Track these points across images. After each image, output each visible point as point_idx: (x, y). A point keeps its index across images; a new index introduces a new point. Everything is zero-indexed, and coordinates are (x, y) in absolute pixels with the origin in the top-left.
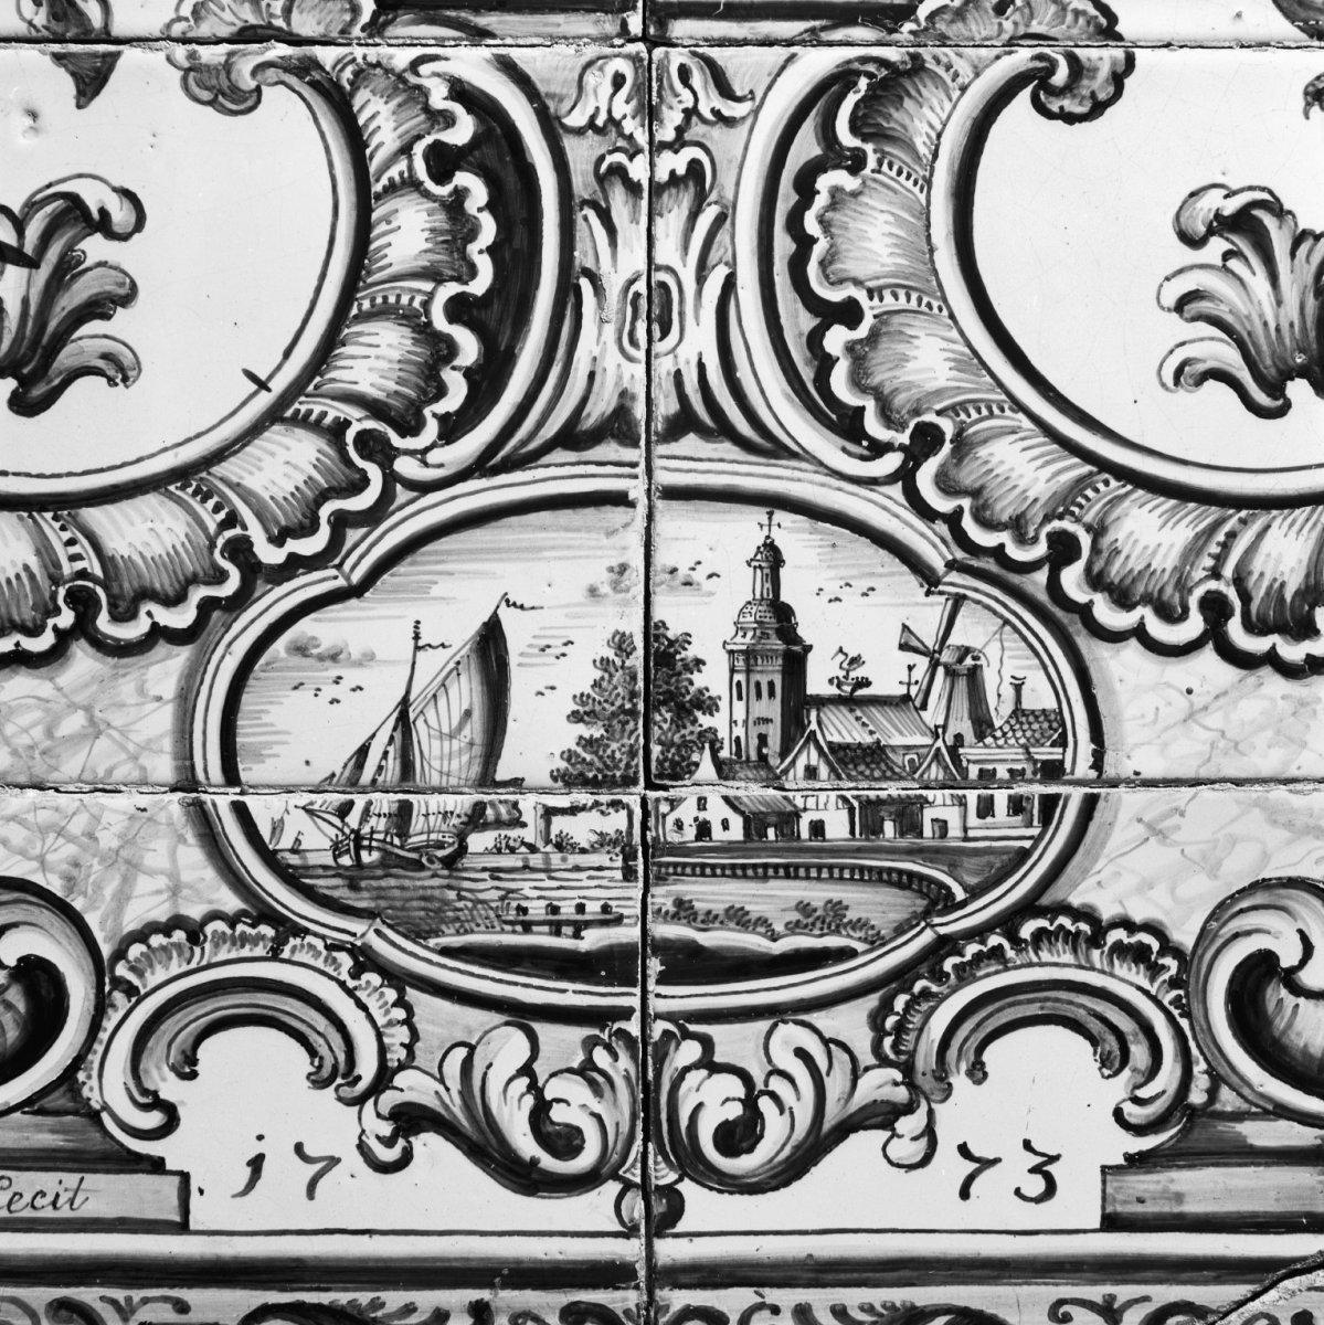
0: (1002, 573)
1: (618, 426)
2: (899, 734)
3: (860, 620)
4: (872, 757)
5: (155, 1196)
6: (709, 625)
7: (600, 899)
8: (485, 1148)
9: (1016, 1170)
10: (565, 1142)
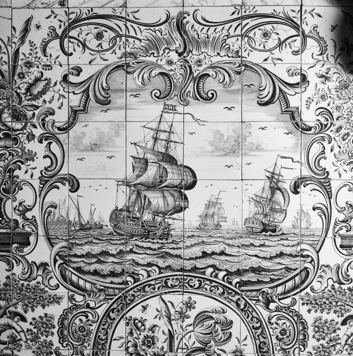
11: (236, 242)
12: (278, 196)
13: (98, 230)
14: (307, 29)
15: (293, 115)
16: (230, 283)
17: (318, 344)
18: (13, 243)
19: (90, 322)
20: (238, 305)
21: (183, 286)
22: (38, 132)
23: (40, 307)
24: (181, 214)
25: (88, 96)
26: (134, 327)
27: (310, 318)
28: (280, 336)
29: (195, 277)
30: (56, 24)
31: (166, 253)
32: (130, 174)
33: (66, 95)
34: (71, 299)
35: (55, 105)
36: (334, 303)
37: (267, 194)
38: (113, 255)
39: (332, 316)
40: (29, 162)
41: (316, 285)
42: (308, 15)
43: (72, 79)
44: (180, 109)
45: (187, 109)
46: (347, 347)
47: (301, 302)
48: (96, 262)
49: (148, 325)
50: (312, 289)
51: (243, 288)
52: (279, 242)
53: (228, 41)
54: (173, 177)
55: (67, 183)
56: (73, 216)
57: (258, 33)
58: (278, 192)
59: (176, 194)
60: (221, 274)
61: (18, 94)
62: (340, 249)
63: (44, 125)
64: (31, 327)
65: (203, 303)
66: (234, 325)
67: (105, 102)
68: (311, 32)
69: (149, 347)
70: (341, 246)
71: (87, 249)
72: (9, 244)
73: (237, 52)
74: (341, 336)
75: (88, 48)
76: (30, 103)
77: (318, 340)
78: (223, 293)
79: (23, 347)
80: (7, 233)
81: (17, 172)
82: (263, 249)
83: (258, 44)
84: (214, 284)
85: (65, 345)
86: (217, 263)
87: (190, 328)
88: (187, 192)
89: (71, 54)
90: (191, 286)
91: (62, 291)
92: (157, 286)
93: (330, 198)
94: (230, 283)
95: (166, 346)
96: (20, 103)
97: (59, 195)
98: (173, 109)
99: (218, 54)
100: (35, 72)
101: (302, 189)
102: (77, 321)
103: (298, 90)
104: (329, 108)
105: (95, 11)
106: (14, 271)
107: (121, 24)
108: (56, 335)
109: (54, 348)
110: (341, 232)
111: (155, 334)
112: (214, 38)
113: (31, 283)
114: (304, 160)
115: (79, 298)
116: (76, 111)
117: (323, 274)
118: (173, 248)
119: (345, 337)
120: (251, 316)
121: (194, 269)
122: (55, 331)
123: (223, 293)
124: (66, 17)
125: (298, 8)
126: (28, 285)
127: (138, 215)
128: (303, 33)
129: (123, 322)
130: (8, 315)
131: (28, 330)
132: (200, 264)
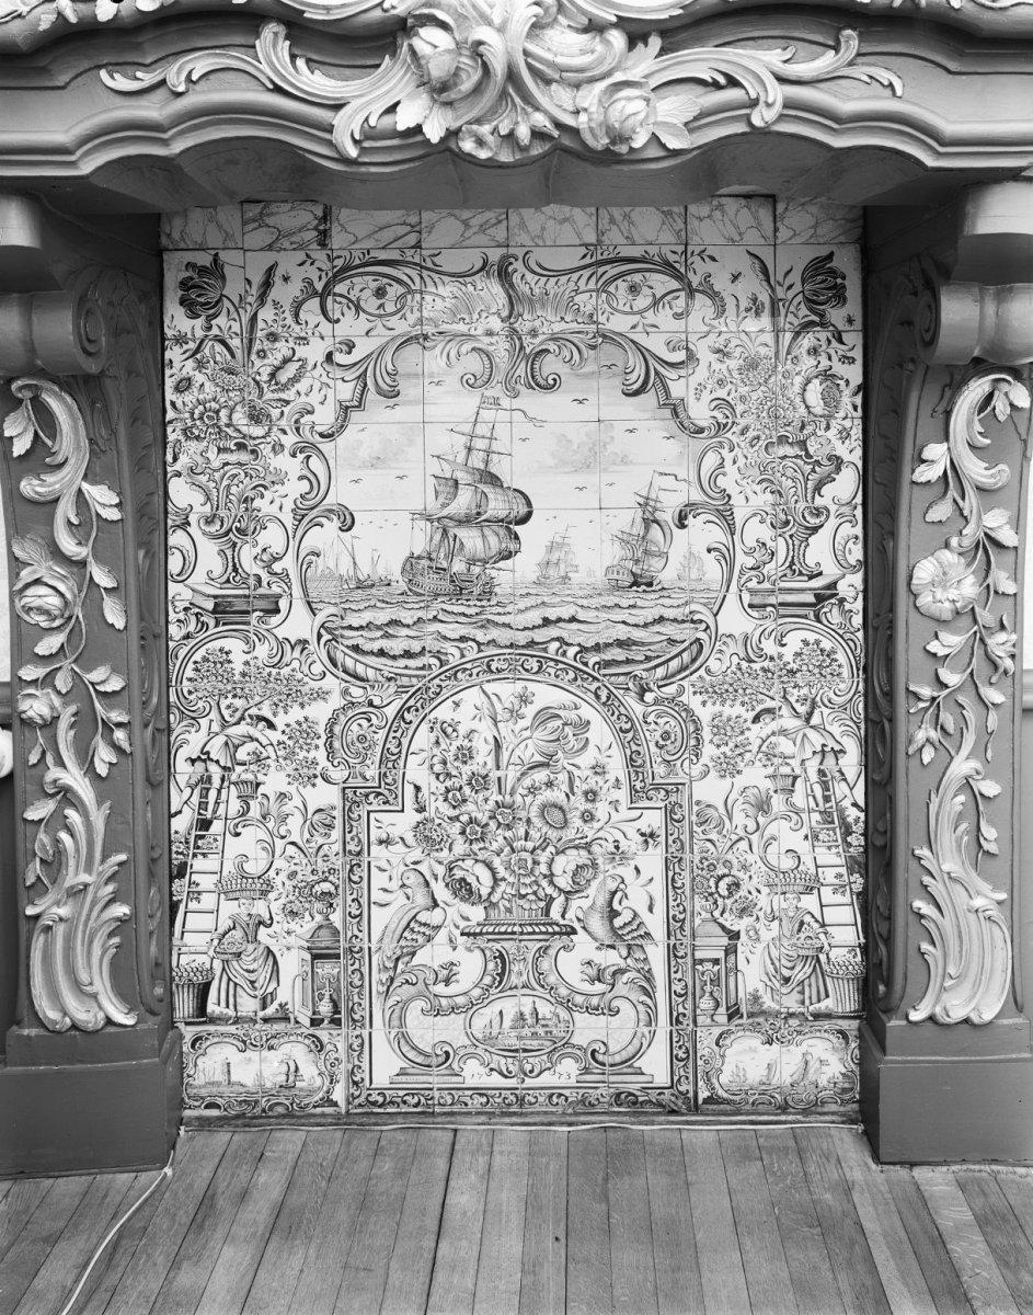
0: (562, 1004)
1: (516, 987)
2: (549, 1023)
3: (545, 1010)
4: (547, 1026)
5: (459, 1079)
6: (527, 1011)
7: (515, 1043)
8: (501, 1073)
9: (565, 1075)
10: (510, 1072)
11: (595, 602)
12: (655, 530)
13: (384, 588)
14: (695, 281)
15: (675, 409)
16: (586, 664)
17: (717, 752)
18: (254, 611)
19: (373, 728)
20: (598, 697)
21: (515, 671)
22: (289, 440)
23: (296, 707)
24: (509, 562)
25: (365, 384)
26: (441, 735)
27: (705, 714)
28: (661, 742)
29: (532, 656)
30: (313, 274)
31: (488, 621)
32: (433, 506)
33: (331, 383)
34: (345, 692)
35: (314, 399)
36: (740, 691)
37: (639, 529)
38: (408, 626)
39: (738, 710)
40: (277, 487)
41: (713, 664)
42: (697, 259)
43: (339, 358)
44: (505, 402)
45: (516, 403)
46: (760, 755)
47: (692, 690)
48: (382, 637)
49: (462, 730)
50: (708, 671)
51: (603, 672)
52: (660, 601)
53: (577, 299)
54: (497, 506)
55: (335, 518)
56: (345, 568)
57: (622, 285)
58: (655, 525)
59: (502, 532)
60: (572, 651)
61: (257, 383)
62: (749, 610)
63: (298, 429)
64: (285, 738)
65: (545, 695)
66: (592, 726)
67: (392, 394)
68: (700, 284)
69: (465, 763)
70: (751, 606)
71: (366, 617)
72: (247, 612)
73: (591, 316)
74: (751, 740)
75: (364, 311)
76: (276, 396)
77: (718, 746)
78: (575, 679)
79: (272, 769)
80: (245, 596)
81: (257, 503)
82: (633, 611)
83: (621, 303)
84: (561, 666)
85: (336, 763)
86: (565, 635)
87: (527, 734)
88: (518, 529)
89: (338, 321)
90: (527, 670)
91: (330, 682)
92: (475, 671)
93: (732, 534)
94: (586, 664)
95: (491, 763)
96: (261, 395)
97: (324, 536)
98: (496, 401)
99: (562, 318)
100: (282, 349)
101: (690, 521)
102: (355, 727)
103: (683, 372)
104: (729, 399)
105: (373, 254)
106: (255, 654)
107: (414, 273)
108: (322, 748)
109: (319, 768)
110: (749, 585)
111: (474, 744)
112: (556, 295)
113: (282, 671)
114: (693, 477)
115: (356, 692)
116: (347, 407)
117: (724, 648)
118: (499, 614)
119: (759, 742)
120: (617, 713)
121: (532, 644)
122: (321, 742)
123: (575, 679)
124: (329, 264)
125: (680, 249)
126: (279, 674)
127: (445, 565)
128: (689, 284)
129: (425, 727)
130: (249, 720)
131: (279, 743)
132: (539, 636)
